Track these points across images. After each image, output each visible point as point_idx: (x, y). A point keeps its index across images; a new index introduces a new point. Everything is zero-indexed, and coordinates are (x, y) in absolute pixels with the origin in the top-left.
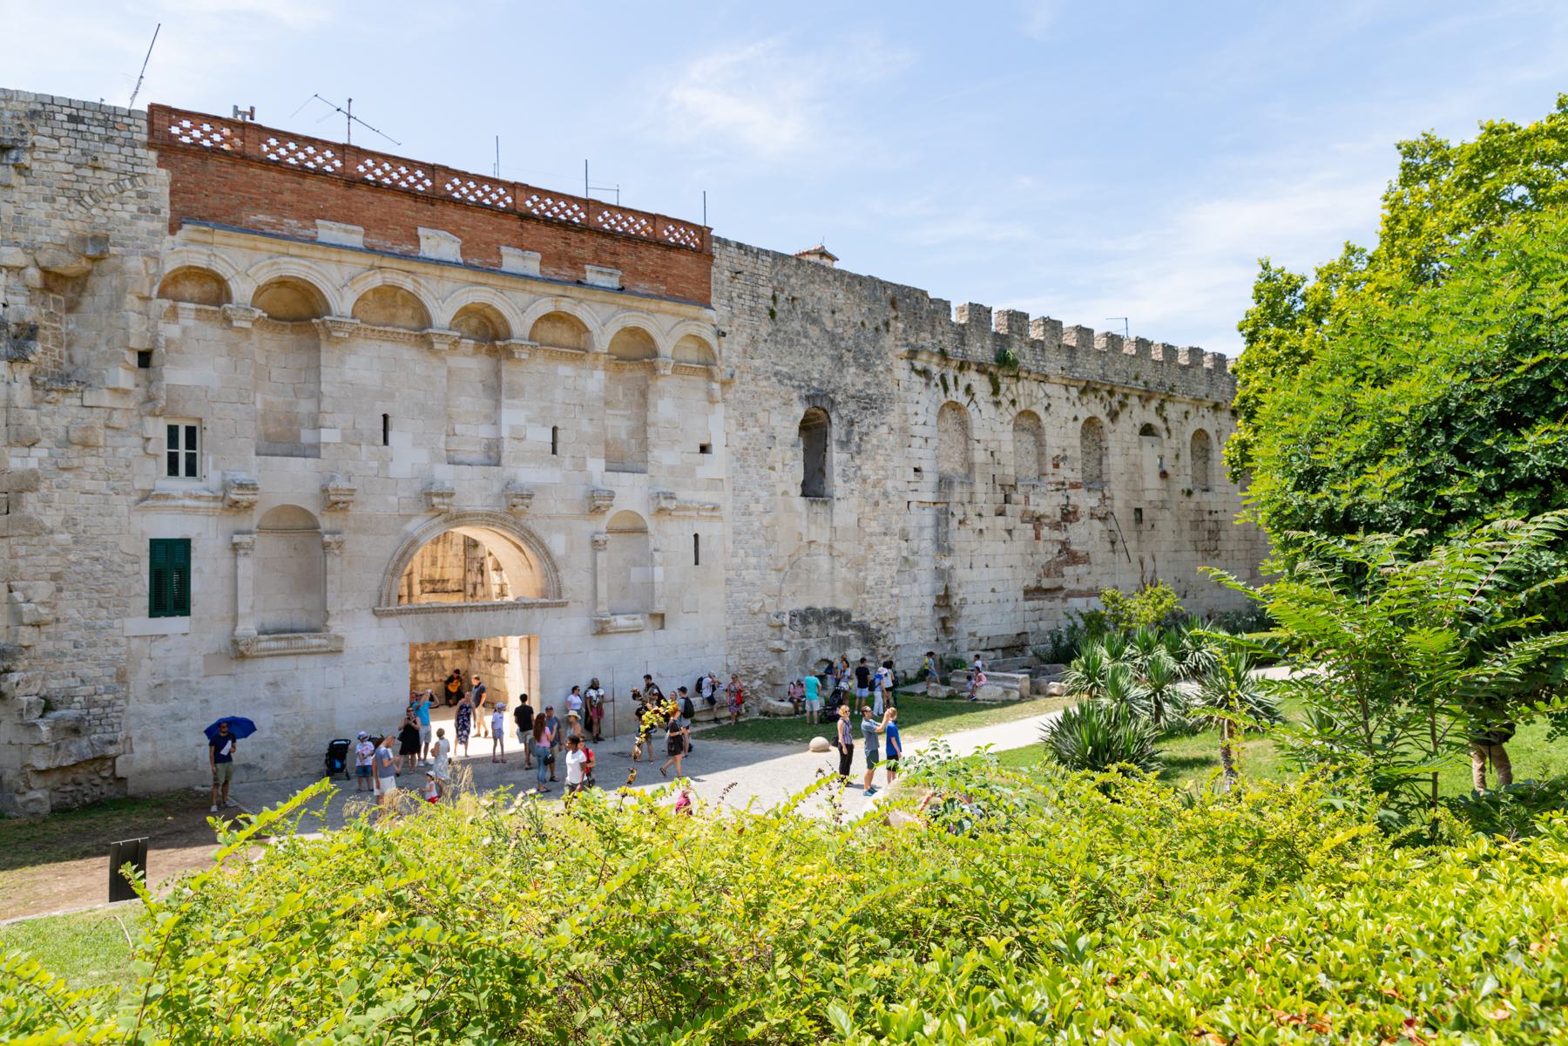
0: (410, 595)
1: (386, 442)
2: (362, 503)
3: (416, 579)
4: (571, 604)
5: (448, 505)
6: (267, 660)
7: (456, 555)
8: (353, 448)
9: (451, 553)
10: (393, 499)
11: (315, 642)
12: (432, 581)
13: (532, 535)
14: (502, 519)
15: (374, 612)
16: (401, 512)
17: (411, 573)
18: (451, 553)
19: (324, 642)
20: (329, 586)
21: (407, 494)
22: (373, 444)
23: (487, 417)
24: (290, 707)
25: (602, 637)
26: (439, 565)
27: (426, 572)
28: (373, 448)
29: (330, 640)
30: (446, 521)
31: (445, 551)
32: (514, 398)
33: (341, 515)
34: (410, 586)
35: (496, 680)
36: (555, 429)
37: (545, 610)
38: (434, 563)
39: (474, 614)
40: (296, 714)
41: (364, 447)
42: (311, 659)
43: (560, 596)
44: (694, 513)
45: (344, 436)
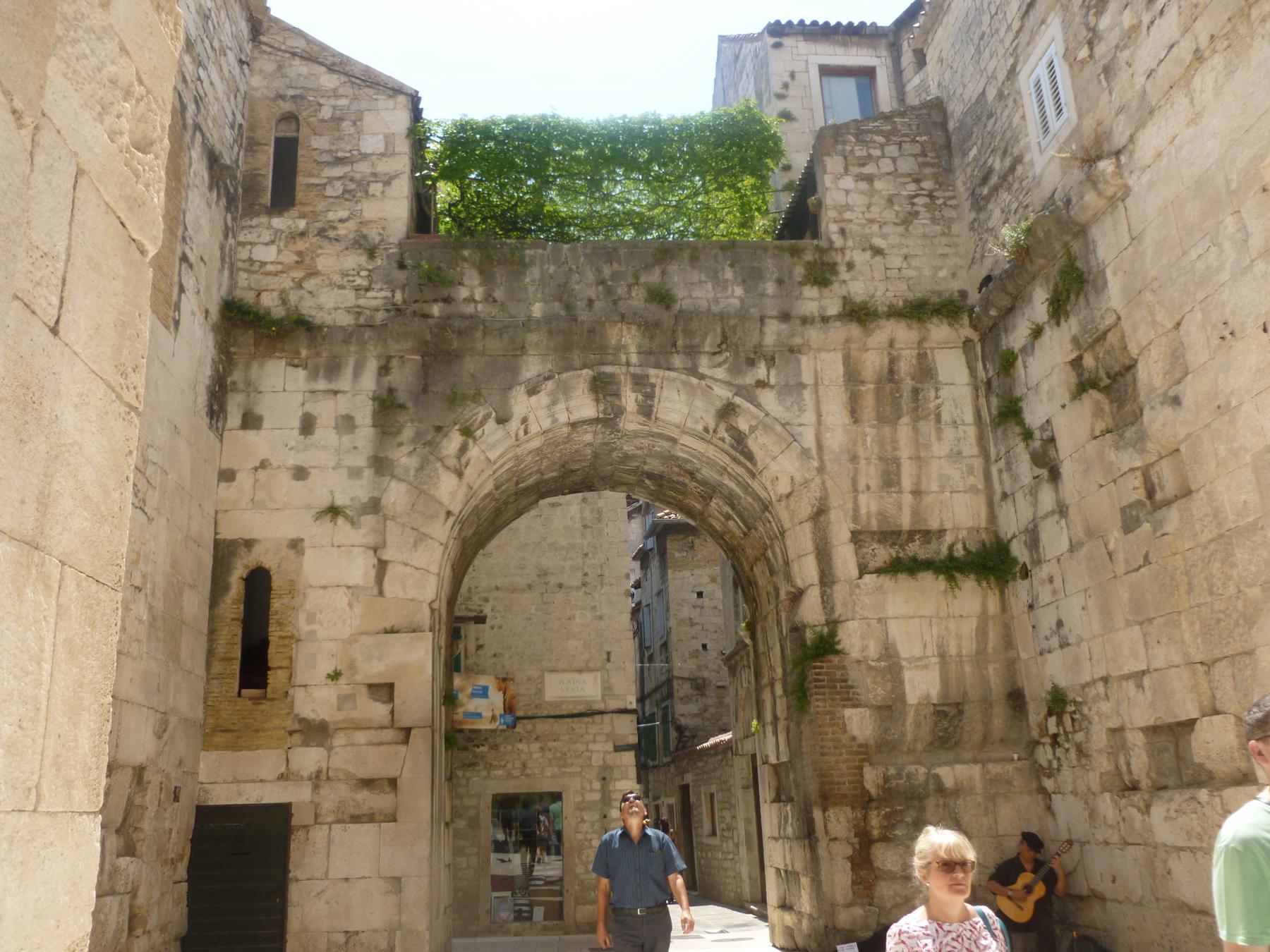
0: (827, 579)
3: (840, 531)
7: (956, 455)
9: (941, 449)
12: (889, 536)
17: (820, 513)
18: (941, 449)
26: (907, 484)
27: (869, 504)
31: (918, 443)
34: (823, 554)
35: (1180, 867)
38: (890, 480)
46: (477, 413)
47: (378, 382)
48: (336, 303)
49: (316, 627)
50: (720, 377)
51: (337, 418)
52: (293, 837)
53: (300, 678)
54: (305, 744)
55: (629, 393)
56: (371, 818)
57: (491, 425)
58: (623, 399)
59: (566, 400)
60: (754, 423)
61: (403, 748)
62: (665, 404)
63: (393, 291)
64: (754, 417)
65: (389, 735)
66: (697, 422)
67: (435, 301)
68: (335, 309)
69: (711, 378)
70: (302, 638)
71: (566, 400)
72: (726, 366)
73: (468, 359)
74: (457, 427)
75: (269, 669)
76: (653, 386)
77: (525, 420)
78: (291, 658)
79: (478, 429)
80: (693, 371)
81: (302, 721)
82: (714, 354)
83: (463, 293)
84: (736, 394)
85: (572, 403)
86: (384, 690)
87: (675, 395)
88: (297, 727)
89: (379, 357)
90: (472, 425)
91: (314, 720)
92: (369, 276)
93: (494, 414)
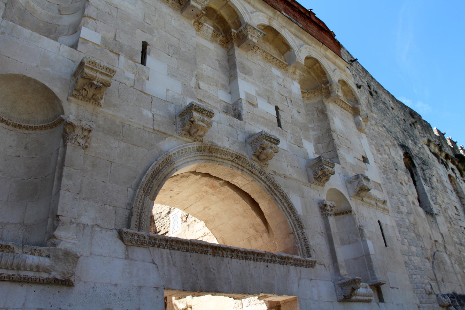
1: (143, 62)
2: (115, 106)
4: (317, 266)
8: (112, 55)
10: (148, 113)
11: (33, 260)
13: (277, 188)
15: (121, 235)
19: (46, 262)
20: (64, 181)
22: (131, 58)
23: (223, 86)
28: (130, 62)
29: (57, 258)
30: (199, 149)
32: (246, 74)
33: (90, 107)
36: (277, 108)
39: (234, 261)
41: (122, 58)
43: (310, 256)
44: (373, 202)
45: (104, 39)
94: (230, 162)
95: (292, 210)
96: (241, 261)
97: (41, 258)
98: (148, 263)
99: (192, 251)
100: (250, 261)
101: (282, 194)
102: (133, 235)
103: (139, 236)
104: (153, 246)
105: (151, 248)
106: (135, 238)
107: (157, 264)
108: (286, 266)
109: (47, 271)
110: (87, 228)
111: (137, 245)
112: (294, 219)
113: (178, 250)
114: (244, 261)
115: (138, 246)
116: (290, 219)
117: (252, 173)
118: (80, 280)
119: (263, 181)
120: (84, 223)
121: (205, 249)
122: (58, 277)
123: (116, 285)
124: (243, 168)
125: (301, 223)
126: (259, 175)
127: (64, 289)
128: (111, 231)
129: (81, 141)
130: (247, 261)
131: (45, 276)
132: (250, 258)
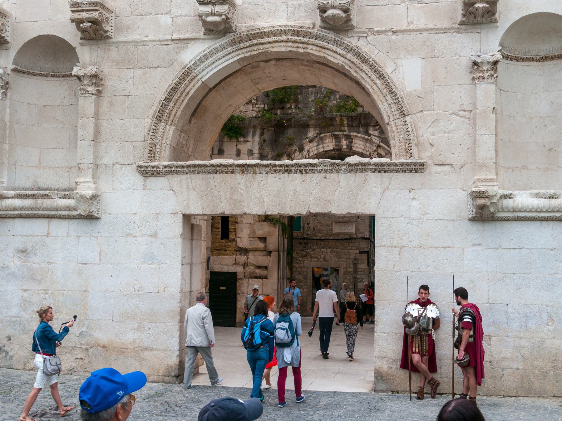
5: (220, 15)
6: (18, 222)
10: (166, 20)
13: (364, 60)
14: (318, 37)
16: (175, 36)
21: (184, 13)
24: (40, 282)
25: (489, 227)
30: (233, 43)
37: (386, 176)
40: (46, 291)
42: (64, 224)
46: (292, 150)
47: (260, 138)
48: (246, 109)
49: (243, 219)
50: (376, 135)
51: (247, 151)
52: (238, 282)
53: (239, 235)
54: (241, 254)
55: (344, 141)
56: (260, 277)
57: (297, 153)
58: (342, 143)
59: (322, 144)
60: (387, 152)
61: (269, 257)
62: (356, 145)
63: (265, 105)
64: (387, 150)
65: (265, 253)
66: (367, 151)
67: (279, 108)
68: (246, 111)
69: (373, 135)
70: (239, 222)
71: (322, 144)
72: (378, 131)
73: (289, 129)
74: (286, 154)
75: (229, 232)
76: (352, 139)
77: (308, 151)
78: (235, 229)
79: (293, 155)
80: (367, 133)
81: (239, 248)
82: (375, 126)
83: (288, 106)
84: (381, 142)
85: (325, 145)
86: (263, 239)
87: (359, 142)
88: (238, 249)
89: (260, 129)
90: (291, 153)
91: (243, 248)
92: (256, 99)
93: (298, 149)
94: (284, 44)
95: (390, 89)
96: (282, 176)
97: (70, 200)
98: (166, 191)
99: (216, 172)
100: (295, 175)
101: (372, 67)
102: (147, 167)
103: (153, 167)
104: (171, 173)
105: (169, 176)
106: (150, 170)
107: (175, 190)
108: (361, 174)
109: (75, 209)
110: (108, 168)
111: (152, 175)
112: (391, 101)
113: (198, 173)
114: (286, 175)
115: (156, 176)
116: (385, 104)
117: (321, 47)
118: (105, 213)
119: (339, 54)
120: (106, 164)
121: (230, 169)
122: (82, 213)
123: (135, 213)
124: (305, 46)
125: (402, 108)
126: (335, 48)
127: (94, 222)
128: (131, 166)
129: (90, 89)
130: (290, 175)
131: (75, 213)
132: (293, 171)
